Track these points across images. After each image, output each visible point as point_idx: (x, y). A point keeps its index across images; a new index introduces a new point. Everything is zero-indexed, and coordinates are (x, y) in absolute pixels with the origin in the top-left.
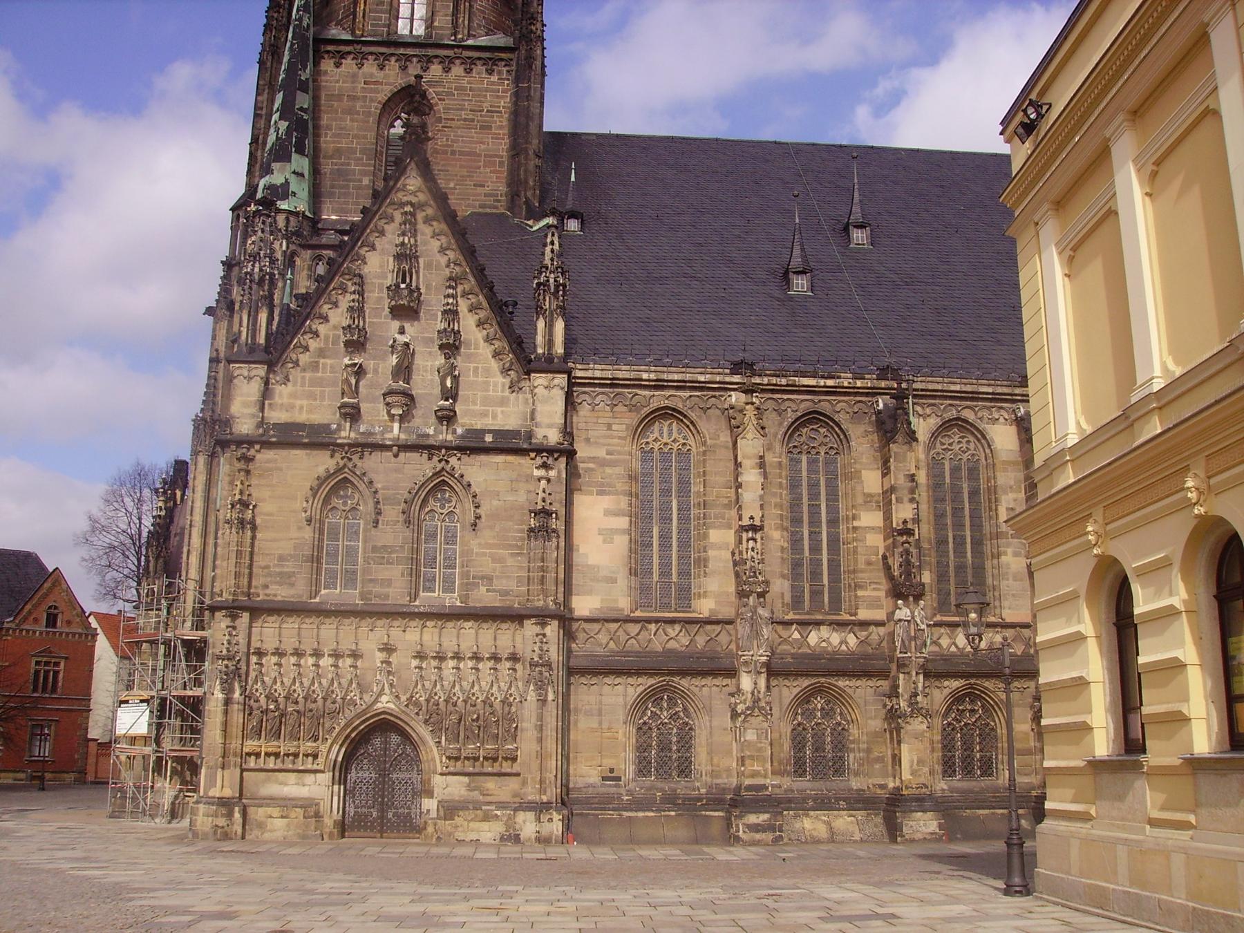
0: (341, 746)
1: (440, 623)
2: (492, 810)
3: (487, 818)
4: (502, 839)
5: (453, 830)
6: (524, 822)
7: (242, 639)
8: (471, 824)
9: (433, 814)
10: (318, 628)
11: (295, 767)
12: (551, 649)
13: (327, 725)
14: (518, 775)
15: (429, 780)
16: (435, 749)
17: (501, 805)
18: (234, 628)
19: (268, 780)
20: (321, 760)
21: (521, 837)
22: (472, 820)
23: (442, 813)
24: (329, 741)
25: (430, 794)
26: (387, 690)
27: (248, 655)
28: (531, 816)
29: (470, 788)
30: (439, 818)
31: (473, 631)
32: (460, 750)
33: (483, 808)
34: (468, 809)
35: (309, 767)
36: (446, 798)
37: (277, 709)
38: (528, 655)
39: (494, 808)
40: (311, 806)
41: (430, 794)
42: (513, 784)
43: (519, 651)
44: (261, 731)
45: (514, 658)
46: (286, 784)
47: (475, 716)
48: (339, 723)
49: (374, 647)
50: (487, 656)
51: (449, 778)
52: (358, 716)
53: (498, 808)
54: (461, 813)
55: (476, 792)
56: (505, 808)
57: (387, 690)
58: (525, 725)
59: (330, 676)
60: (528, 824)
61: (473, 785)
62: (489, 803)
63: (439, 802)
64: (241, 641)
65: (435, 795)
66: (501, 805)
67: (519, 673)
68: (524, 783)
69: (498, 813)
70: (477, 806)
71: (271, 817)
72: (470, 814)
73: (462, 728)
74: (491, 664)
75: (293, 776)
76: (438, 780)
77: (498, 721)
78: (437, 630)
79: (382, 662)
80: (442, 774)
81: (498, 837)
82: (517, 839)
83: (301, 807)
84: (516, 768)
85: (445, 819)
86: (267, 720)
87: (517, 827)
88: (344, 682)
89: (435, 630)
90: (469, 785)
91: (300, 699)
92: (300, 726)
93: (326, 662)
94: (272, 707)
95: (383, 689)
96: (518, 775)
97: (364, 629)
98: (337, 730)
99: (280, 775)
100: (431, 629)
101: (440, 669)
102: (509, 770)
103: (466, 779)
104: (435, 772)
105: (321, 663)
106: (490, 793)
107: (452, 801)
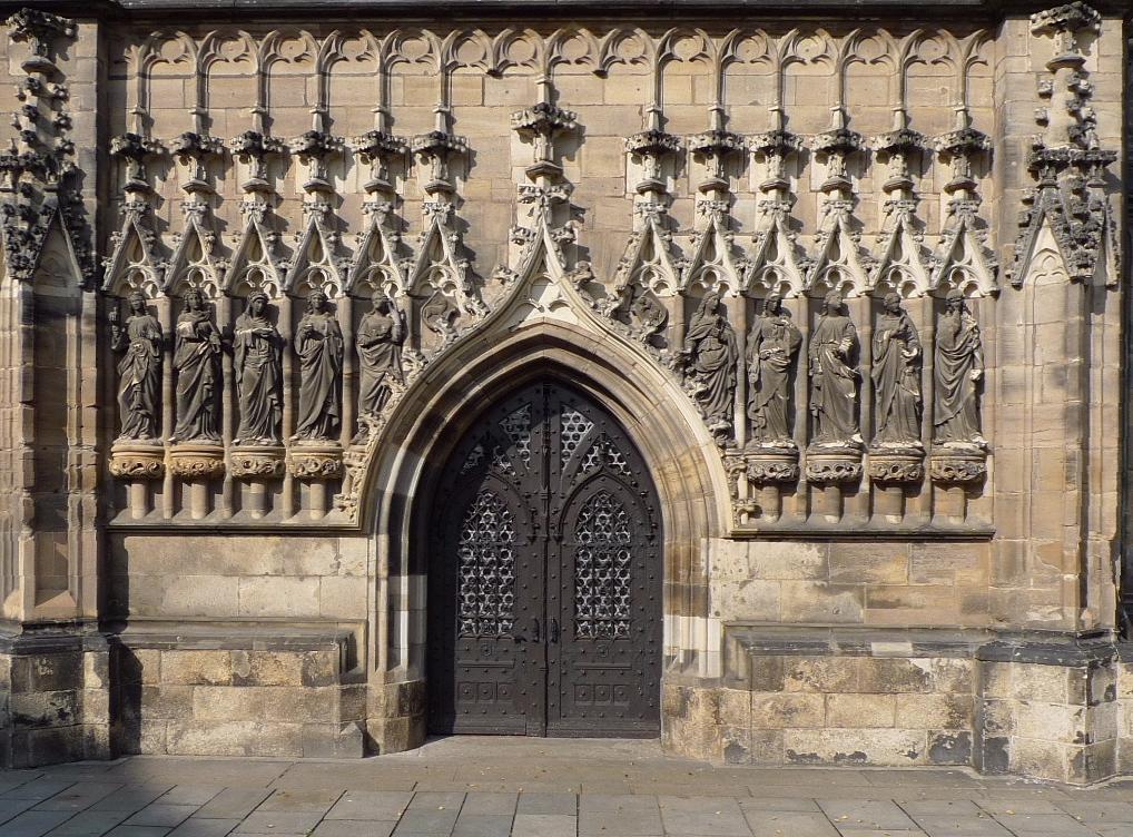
0: (414, 449)
1: (717, 44)
2: (903, 657)
3: (889, 680)
4: (937, 747)
5: (778, 721)
6: (1024, 700)
7: (80, 110)
8: (838, 701)
9: (710, 666)
10: (323, 74)
11: (271, 520)
12: (1099, 117)
13: (367, 380)
14: (983, 537)
15: (693, 555)
16: (712, 455)
17: (934, 641)
18: (53, 74)
19: (189, 562)
20: (351, 495)
21: (1013, 751)
22: (840, 688)
23: (739, 665)
24: (374, 434)
25: (697, 601)
26: (554, 264)
27: (107, 164)
28: (1051, 681)
29: (826, 582)
30: (729, 677)
31: (828, 69)
32: (794, 457)
33: (875, 647)
34: (823, 650)
35: (313, 515)
36: (747, 613)
37: (200, 335)
38: (1023, 134)
39: (906, 647)
40: (320, 643)
41: (697, 601)
42: (966, 569)
43: (984, 122)
44: (158, 406)
45: (972, 150)
46: (247, 576)
47: (845, 346)
48: (401, 378)
49: (508, 129)
50: (883, 143)
51: (759, 547)
52: (461, 351)
53: (924, 649)
54: (803, 665)
55: (847, 595)
56: (943, 648)
57: (554, 264)
58: (1015, 371)
59: (367, 224)
60: (1038, 706)
61: (834, 572)
62: (894, 632)
63: (727, 627)
64: (75, 115)
65: (715, 605)
66: (934, 641)
67: (988, 206)
68: (1012, 566)
69: (924, 664)
70: (853, 641)
71: (203, 682)
72: (833, 668)
73: (800, 386)
74: (894, 169)
75: (264, 550)
76: (723, 559)
77: (918, 361)
78: (710, 68)
79: (533, 174)
80: (738, 537)
81: (924, 745)
82: (993, 753)
83: (293, 646)
84: (980, 514)
85: (752, 686)
86: (175, 372)
87: (997, 714)
88: (415, 241)
89: (698, 67)
90: (822, 572)
91: (281, 301)
92: (278, 387)
93: (357, 179)
94: (185, 325)
95: (539, 263)
96: (983, 537)
97: (471, 74)
98: (397, 395)
99: (227, 544)
100: (688, 67)
101: (721, 189)
102: (955, 523)
103: (811, 553)
104: (710, 531)
105: (341, 187)
106: (892, 596)
107: (768, 623)
